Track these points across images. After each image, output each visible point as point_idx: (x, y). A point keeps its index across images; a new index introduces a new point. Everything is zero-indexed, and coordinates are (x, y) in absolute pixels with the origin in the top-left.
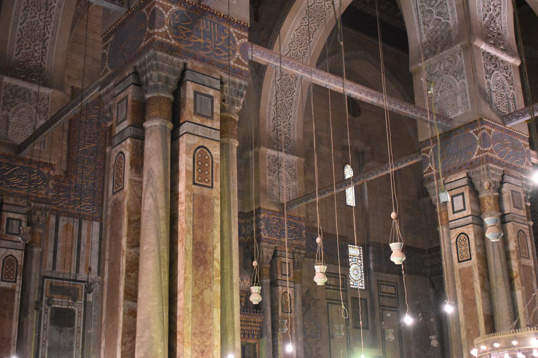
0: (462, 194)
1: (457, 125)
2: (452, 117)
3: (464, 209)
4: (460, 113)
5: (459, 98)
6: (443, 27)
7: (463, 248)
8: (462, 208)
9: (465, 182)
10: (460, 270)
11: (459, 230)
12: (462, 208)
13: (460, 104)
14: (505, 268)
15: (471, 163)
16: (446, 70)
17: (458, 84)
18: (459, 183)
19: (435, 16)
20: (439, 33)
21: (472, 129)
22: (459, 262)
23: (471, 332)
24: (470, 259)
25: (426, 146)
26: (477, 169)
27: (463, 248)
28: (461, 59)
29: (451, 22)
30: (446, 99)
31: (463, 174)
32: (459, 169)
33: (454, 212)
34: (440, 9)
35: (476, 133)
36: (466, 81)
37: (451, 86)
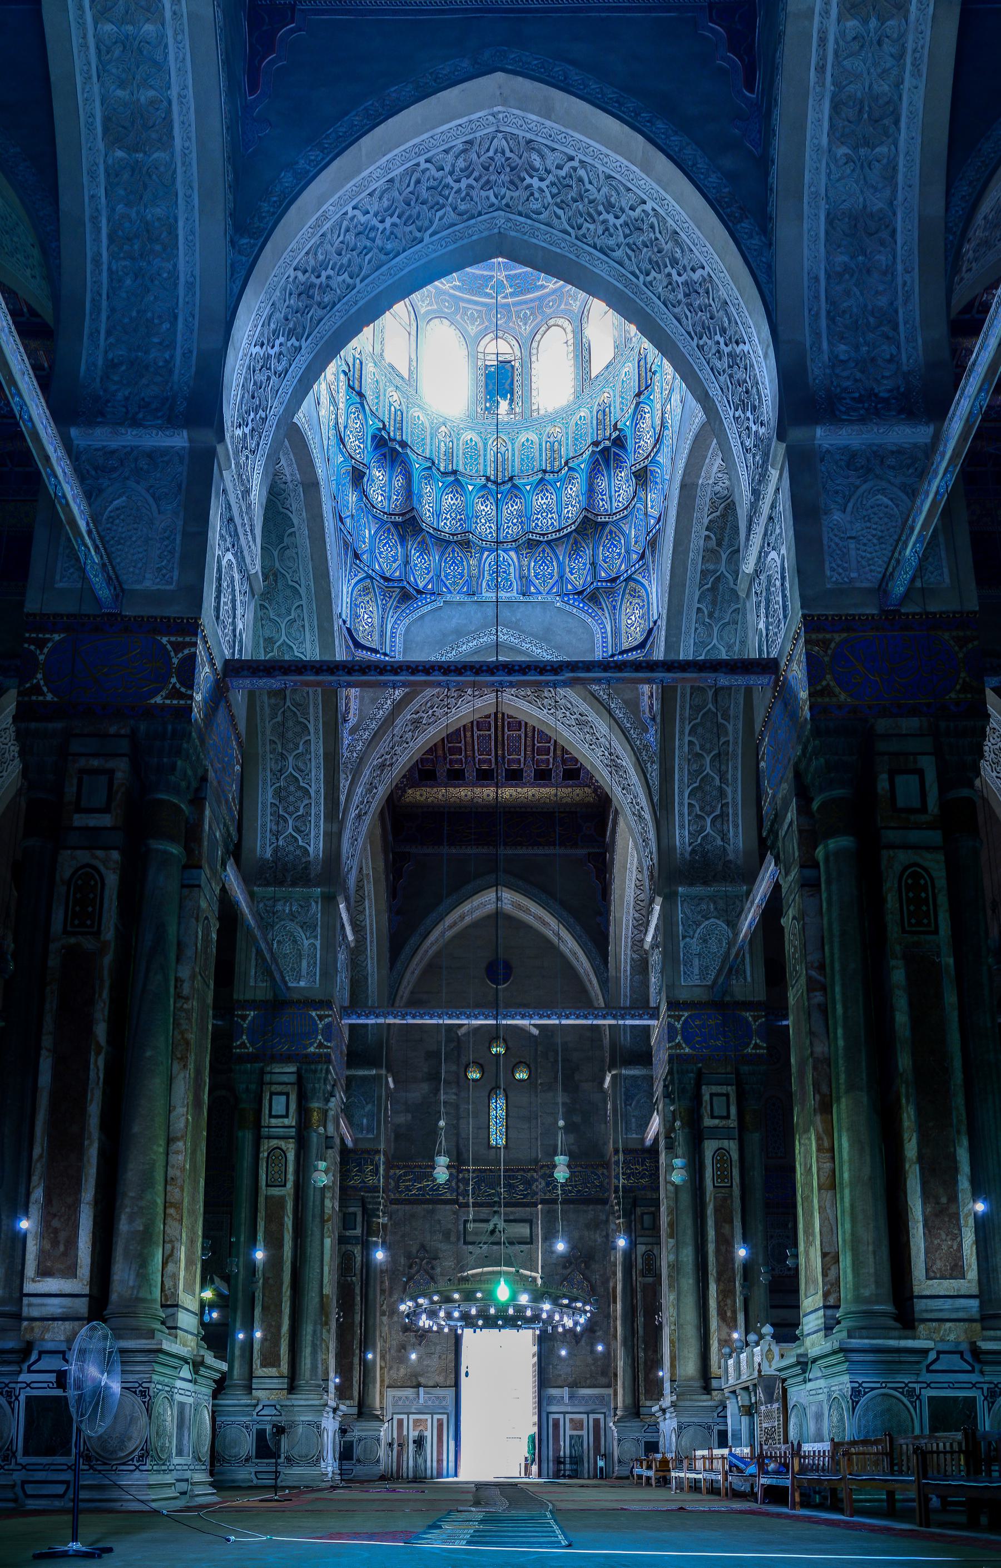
0: (287, 1095)
1: (295, 996)
2: (290, 985)
3: (287, 1116)
4: (302, 984)
5: (304, 963)
6: (298, 852)
7: (277, 1169)
8: (284, 1113)
9: (293, 1078)
10: (267, 1197)
11: (274, 1143)
12: (284, 1113)
13: (304, 972)
14: (371, 1323)
15: (307, 1056)
16: (292, 916)
17: (306, 943)
18: (285, 1079)
19: (290, 830)
20: (291, 857)
21: (315, 1010)
22: (267, 1186)
23: (271, 1281)
24: (285, 1186)
25: (244, 1008)
26: (313, 1067)
27: (277, 1169)
28: (316, 909)
29: (311, 850)
30: (285, 956)
31: (293, 1069)
32: (287, 1059)
33: (271, 1116)
34: (298, 824)
35: (321, 1018)
36: (318, 943)
37: (295, 942)
